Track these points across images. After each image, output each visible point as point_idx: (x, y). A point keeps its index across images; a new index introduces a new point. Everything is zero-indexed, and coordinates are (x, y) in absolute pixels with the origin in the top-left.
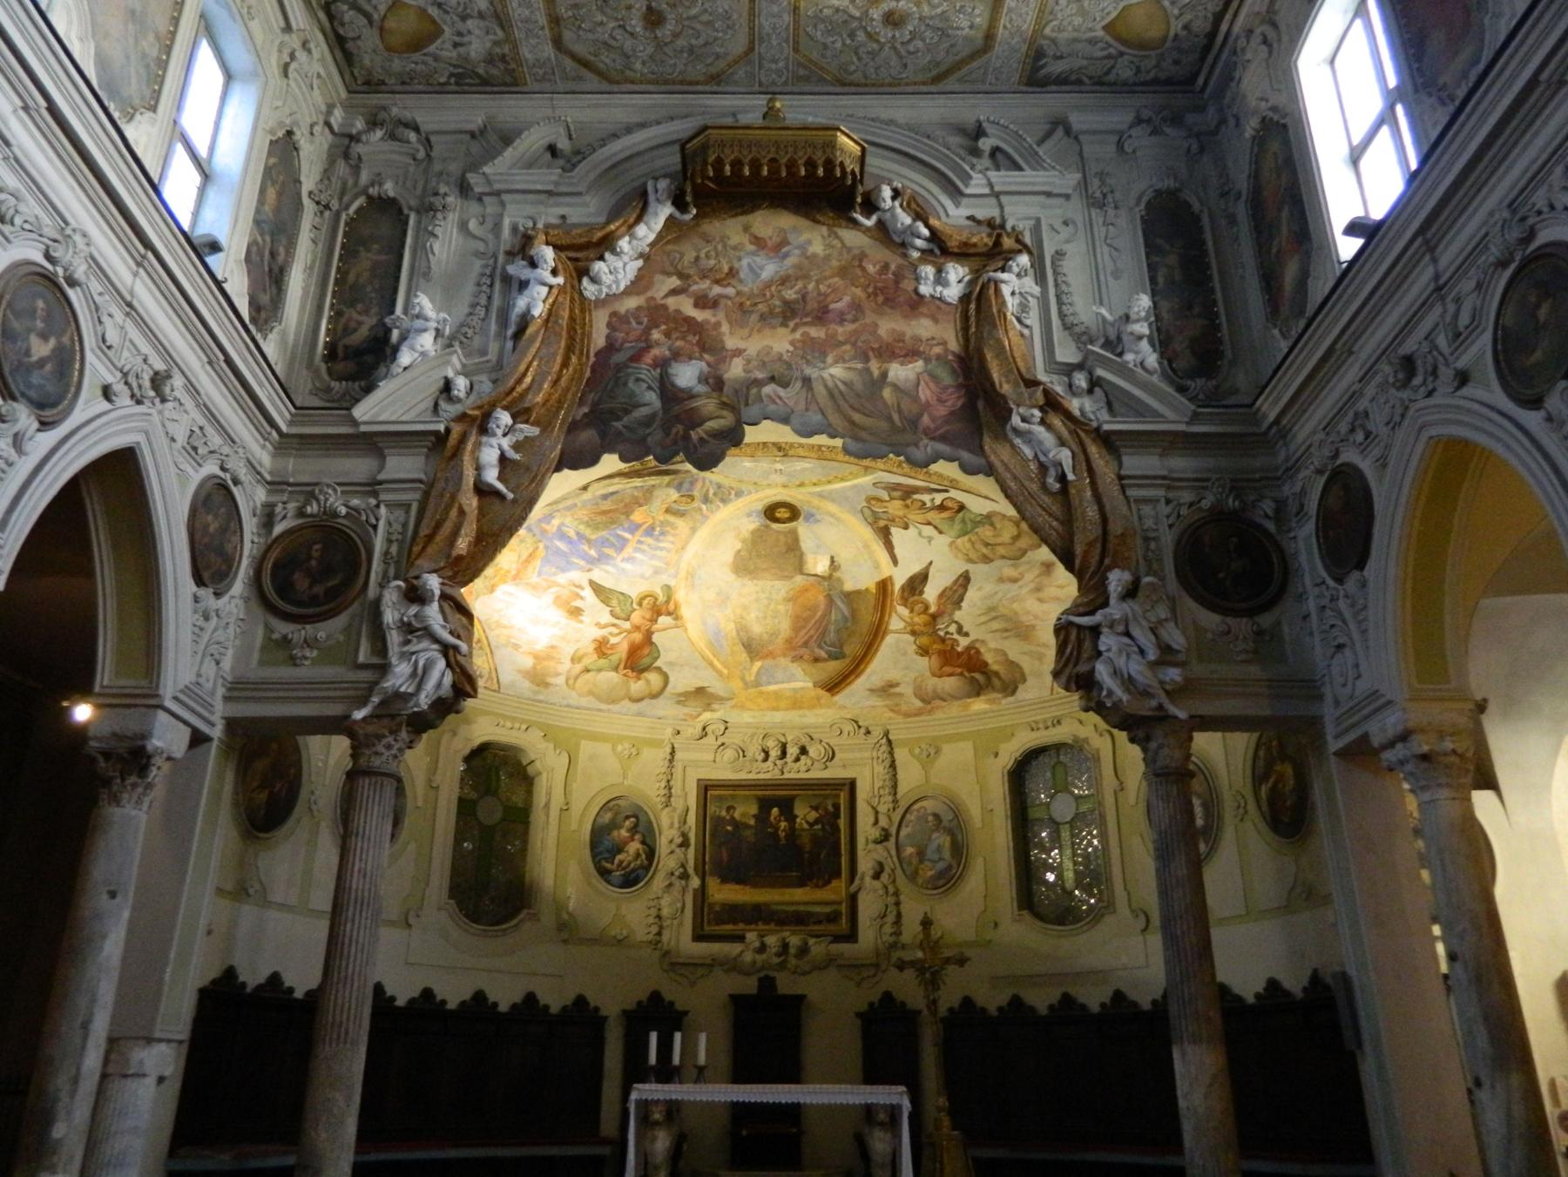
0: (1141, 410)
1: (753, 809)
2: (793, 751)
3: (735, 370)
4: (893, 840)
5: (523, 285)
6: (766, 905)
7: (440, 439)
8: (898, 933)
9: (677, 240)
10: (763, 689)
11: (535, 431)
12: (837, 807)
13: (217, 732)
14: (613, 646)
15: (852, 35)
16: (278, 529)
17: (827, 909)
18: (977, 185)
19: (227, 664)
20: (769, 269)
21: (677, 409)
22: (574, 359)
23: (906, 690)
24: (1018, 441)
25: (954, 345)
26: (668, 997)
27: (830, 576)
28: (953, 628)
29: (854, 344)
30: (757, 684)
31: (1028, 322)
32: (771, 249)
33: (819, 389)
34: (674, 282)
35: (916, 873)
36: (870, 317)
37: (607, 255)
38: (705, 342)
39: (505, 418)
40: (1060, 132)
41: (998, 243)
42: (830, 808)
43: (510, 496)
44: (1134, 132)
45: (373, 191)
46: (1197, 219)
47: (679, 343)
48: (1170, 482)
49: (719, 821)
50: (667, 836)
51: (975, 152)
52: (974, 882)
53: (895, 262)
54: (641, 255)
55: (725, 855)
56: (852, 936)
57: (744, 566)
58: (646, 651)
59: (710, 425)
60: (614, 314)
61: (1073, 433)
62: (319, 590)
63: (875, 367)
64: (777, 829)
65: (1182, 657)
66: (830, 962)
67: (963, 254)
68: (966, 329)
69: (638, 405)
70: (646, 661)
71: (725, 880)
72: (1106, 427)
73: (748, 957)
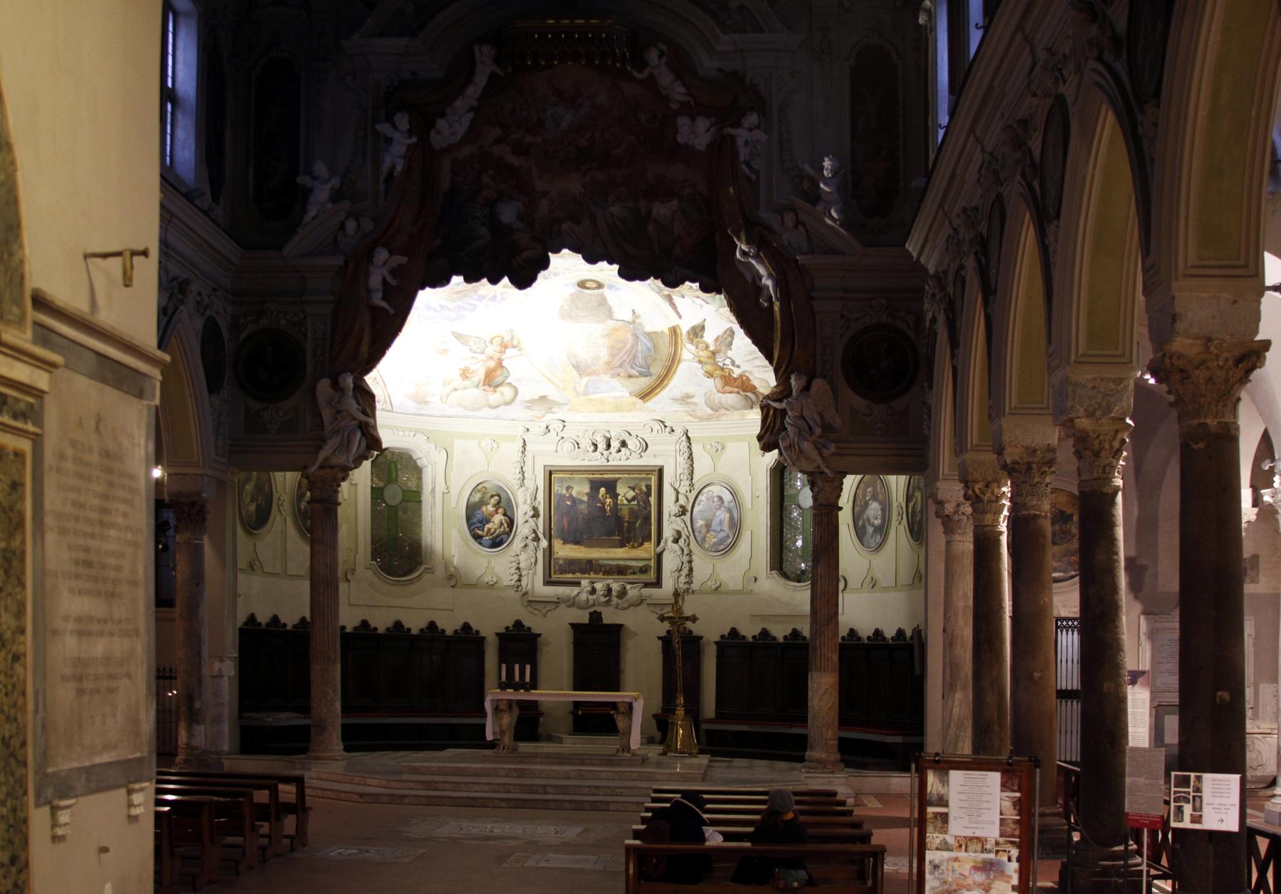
1: (586, 489)
2: (615, 444)
4: (688, 514)
6: (597, 560)
8: (689, 583)
10: (592, 397)
11: (404, 260)
12: (649, 487)
14: (473, 372)
17: (641, 564)
23: (699, 399)
26: (527, 624)
27: (634, 322)
28: (728, 362)
30: (586, 393)
31: (756, 167)
34: (497, 132)
35: (704, 539)
42: (644, 489)
43: (392, 312)
49: (562, 497)
50: (522, 512)
52: (743, 547)
54: (472, 109)
55: (565, 523)
56: (658, 583)
57: (570, 313)
58: (499, 372)
59: (527, 254)
64: (604, 504)
66: (641, 601)
70: (499, 380)
71: (566, 542)
73: (584, 597)
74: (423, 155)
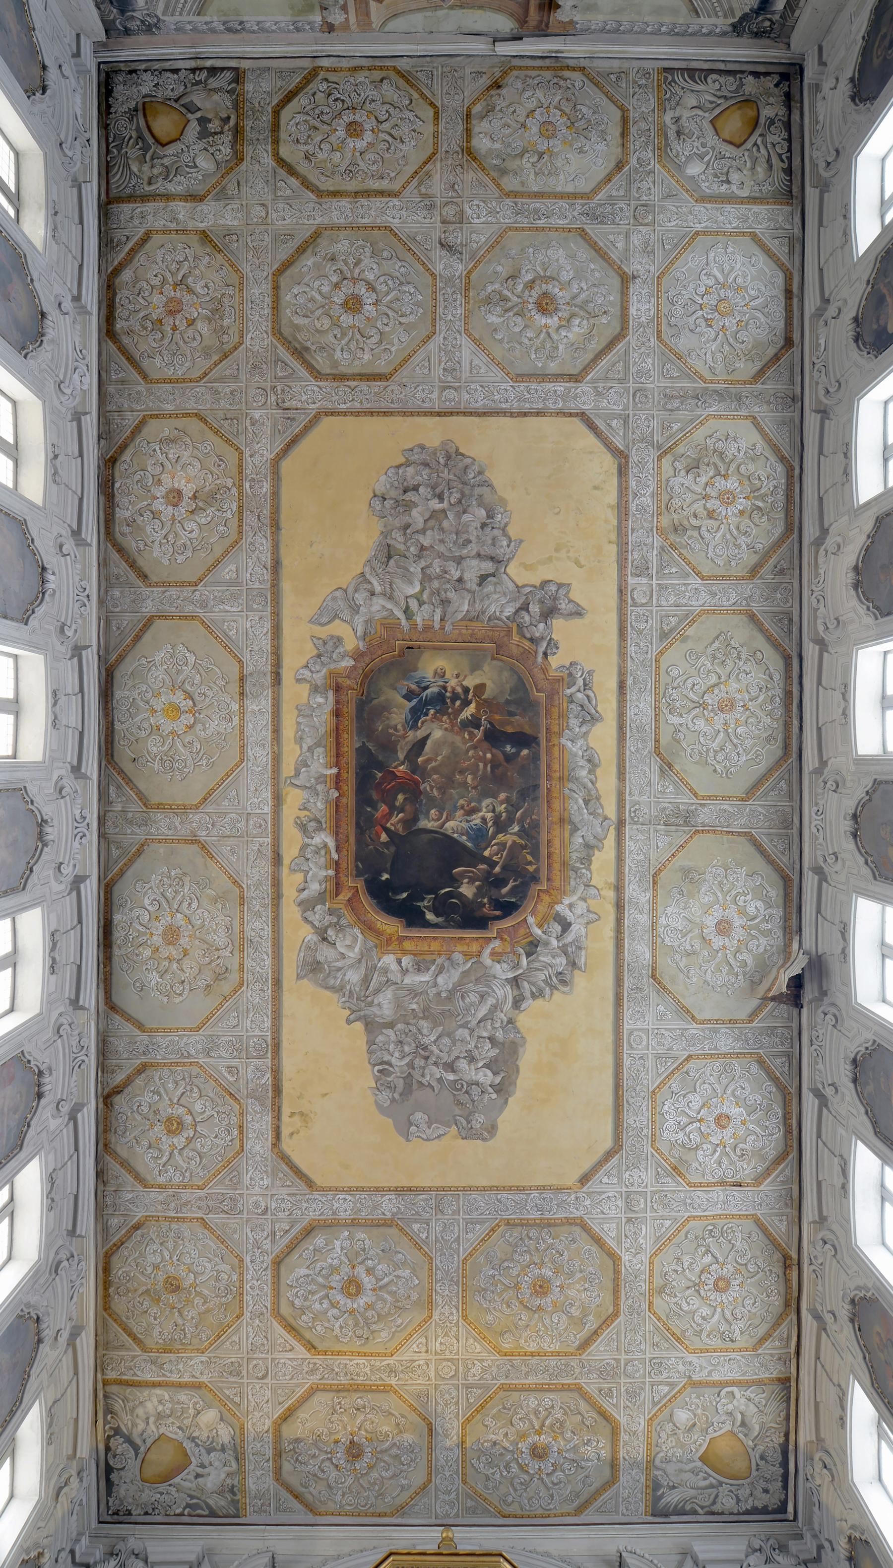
15: (507, 1467)
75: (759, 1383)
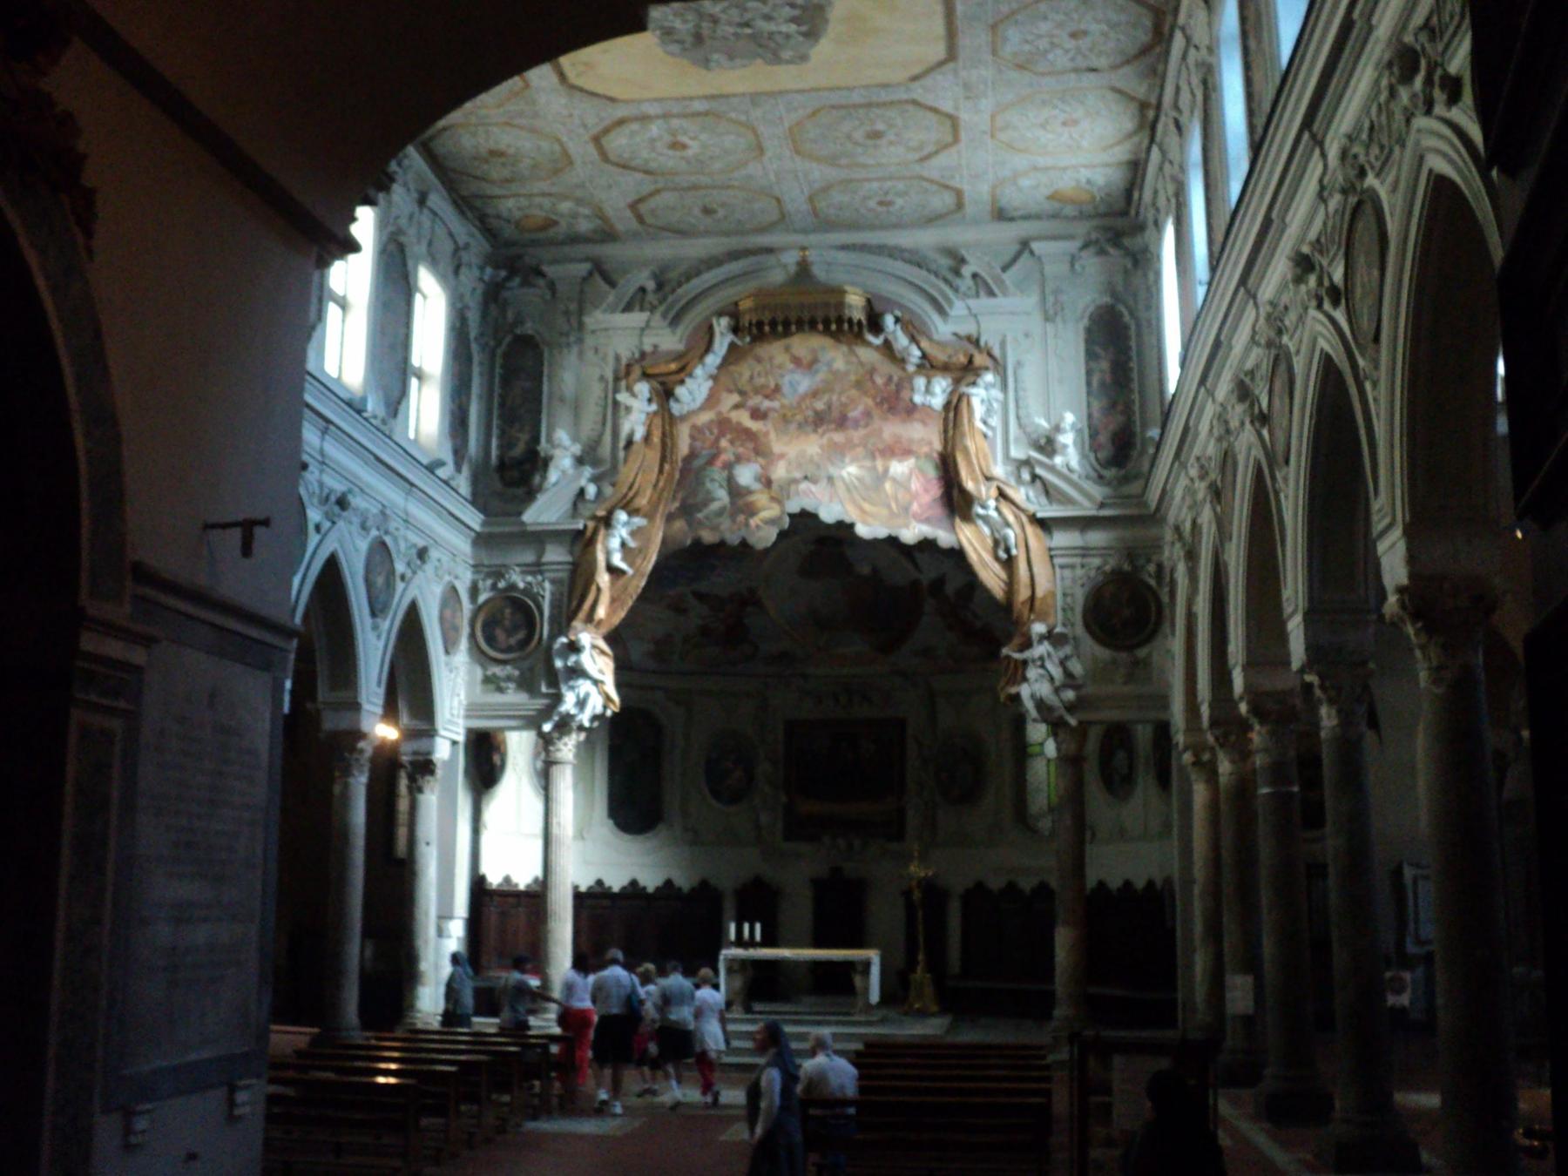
0: (1067, 500)
3: (780, 472)
5: (628, 409)
7: (579, 534)
9: (737, 361)
13: (461, 738)
16: (482, 598)
18: (958, 308)
19: (462, 697)
20: (804, 383)
21: (740, 502)
22: (667, 467)
24: (980, 522)
25: (938, 446)
29: (865, 446)
32: (803, 368)
33: (839, 484)
34: (735, 398)
36: (877, 423)
37: (688, 381)
38: (759, 449)
39: (622, 516)
40: (1026, 255)
41: (970, 361)
43: (630, 571)
44: (1084, 254)
45: (518, 331)
46: (1127, 328)
47: (741, 450)
48: (1085, 552)
51: (957, 272)
53: (896, 373)
59: (765, 514)
60: (694, 427)
61: (1016, 517)
62: (513, 641)
63: (879, 464)
65: (1080, 682)
67: (945, 368)
68: (945, 431)
69: (713, 500)
72: (1039, 515)
74: (666, 420)
75: (1107, 165)
